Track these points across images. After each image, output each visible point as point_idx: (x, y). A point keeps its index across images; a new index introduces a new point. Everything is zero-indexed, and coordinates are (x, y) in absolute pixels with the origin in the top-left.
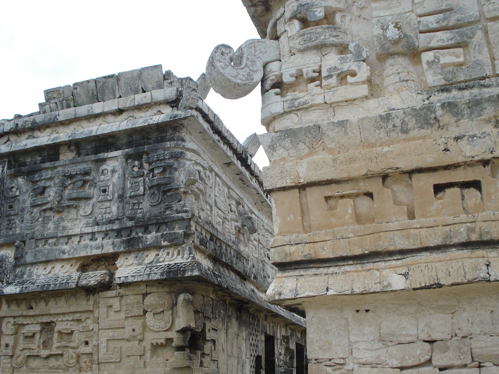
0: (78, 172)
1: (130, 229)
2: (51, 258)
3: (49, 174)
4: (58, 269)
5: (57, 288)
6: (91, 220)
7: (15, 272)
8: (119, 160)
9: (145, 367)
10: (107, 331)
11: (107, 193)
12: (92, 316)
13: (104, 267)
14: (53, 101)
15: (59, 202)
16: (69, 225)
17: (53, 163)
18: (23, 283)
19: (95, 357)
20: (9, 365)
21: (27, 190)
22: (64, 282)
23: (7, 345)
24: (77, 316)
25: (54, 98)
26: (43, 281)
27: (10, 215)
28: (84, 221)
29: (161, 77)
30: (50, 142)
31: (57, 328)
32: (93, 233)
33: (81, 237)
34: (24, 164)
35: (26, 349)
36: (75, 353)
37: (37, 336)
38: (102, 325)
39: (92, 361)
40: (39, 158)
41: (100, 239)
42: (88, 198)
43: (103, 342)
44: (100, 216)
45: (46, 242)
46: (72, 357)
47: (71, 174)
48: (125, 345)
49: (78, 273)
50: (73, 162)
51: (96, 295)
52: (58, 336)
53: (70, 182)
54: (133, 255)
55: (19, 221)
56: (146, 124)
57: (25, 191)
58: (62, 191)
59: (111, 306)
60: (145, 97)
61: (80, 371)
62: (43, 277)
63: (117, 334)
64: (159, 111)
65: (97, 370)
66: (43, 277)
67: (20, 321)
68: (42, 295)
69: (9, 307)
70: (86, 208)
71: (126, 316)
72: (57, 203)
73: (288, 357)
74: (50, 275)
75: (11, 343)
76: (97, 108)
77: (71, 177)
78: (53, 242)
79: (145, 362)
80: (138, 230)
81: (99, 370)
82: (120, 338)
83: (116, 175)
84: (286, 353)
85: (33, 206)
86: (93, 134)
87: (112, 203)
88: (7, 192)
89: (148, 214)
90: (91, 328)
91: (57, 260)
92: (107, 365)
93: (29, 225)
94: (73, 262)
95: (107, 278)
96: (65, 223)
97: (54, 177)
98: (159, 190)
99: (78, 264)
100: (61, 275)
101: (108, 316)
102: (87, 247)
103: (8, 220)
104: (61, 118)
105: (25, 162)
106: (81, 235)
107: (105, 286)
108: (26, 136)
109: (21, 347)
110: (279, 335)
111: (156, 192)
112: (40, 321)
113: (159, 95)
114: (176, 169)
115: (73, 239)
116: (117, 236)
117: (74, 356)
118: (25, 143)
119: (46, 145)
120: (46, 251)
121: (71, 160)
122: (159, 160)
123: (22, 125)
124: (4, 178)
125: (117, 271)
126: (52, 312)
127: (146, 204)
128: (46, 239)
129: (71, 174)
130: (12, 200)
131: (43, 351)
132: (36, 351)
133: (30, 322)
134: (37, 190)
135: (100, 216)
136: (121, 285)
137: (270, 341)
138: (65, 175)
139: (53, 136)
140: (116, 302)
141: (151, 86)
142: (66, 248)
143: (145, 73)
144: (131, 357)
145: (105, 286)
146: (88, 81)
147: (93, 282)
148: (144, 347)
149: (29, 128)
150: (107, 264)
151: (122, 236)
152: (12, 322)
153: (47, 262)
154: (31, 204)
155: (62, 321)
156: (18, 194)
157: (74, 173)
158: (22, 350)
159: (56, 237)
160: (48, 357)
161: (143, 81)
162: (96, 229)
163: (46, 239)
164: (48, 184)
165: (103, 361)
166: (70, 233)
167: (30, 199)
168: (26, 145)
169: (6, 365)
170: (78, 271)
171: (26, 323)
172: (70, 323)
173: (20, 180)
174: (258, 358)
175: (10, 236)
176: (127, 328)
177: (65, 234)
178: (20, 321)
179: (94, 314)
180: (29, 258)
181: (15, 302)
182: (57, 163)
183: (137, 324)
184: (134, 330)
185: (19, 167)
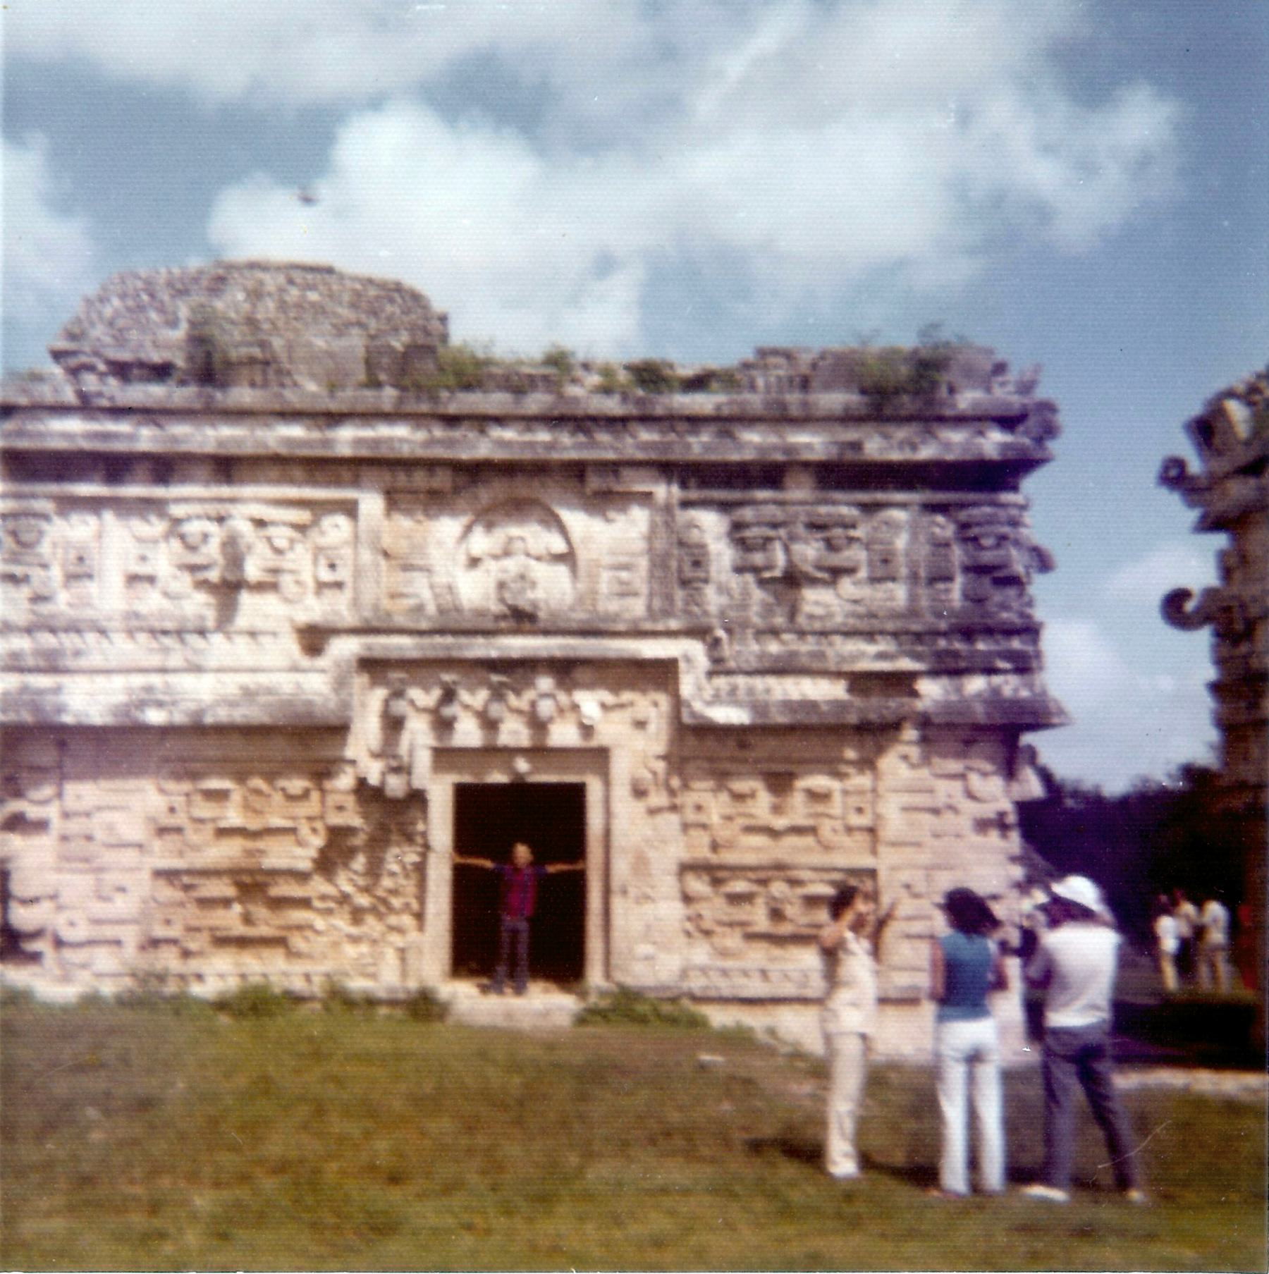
48: (927, 818)
126: (795, 755)
183: (957, 786)
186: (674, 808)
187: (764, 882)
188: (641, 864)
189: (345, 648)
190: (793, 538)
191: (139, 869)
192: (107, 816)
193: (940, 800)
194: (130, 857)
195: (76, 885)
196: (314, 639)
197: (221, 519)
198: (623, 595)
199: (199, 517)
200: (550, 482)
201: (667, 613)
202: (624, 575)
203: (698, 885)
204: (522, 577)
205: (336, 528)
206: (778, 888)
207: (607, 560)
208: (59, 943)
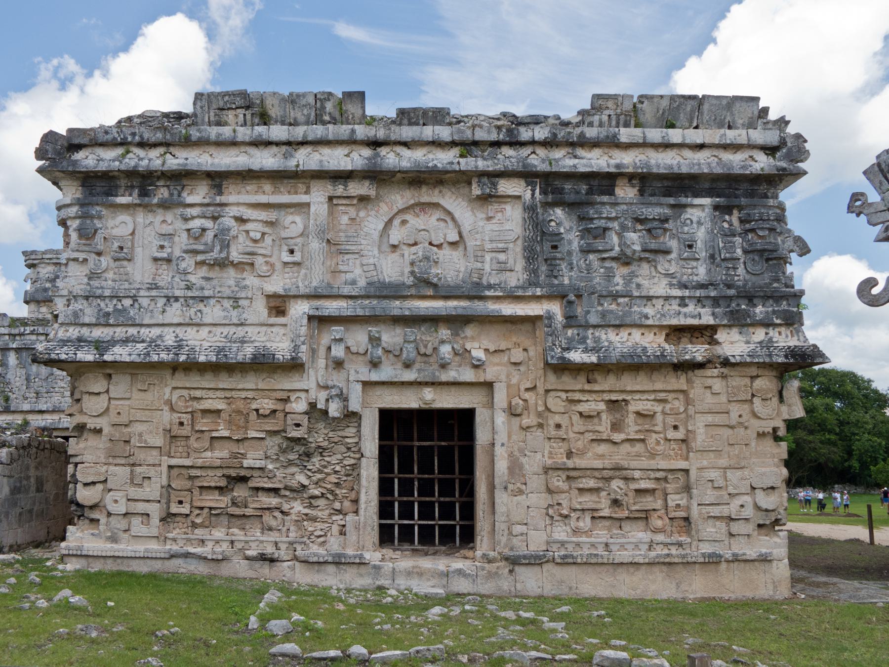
1: (731, 298)
2: (628, 322)
8: (707, 210)
11: (694, 250)
14: (607, 112)
20: (562, 450)
21: (571, 228)
24: (662, 395)
25: (607, 108)
27: (555, 259)
28: (665, 281)
29: (756, 113)
31: (632, 408)
32: (682, 298)
35: (590, 431)
37: (604, 416)
42: (667, 252)
53: (639, 227)
54: (735, 331)
55: (566, 268)
56: (748, 172)
60: (739, 136)
64: (751, 157)
66: (619, 345)
67: (577, 396)
70: (664, 265)
76: (675, 135)
80: (740, 301)
83: (703, 229)
86: (676, 170)
87: (700, 262)
89: (750, 283)
90: (682, 410)
96: (639, 280)
98: (761, 256)
99: (664, 333)
102: (679, 313)
104: (623, 139)
105: (563, 189)
106: (667, 298)
111: (757, 258)
112: (607, 398)
113: (759, 136)
114: (780, 233)
115: (654, 301)
122: (761, 220)
123: (563, 137)
124: (536, 206)
126: (629, 388)
127: (741, 271)
128: (615, 296)
133: (590, 399)
139: (612, 162)
141: (741, 121)
142: (649, 310)
143: (738, 105)
146: (662, 97)
151: (719, 306)
152: (565, 398)
154: (580, 247)
157: (651, 217)
158: (582, 433)
161: (732, 114)
162: (687, 293)
163: (615, 296)
166: (651, 294)
167: (577, 239)
168: (575, 166)
171: (585, 399)
173: (559, 211)
178: (577, 396)
186: (540, 426)
187: (608, 479)
189: (300, 309)
190: (624, 228)
192: (138, 428)
193: (734, 418)
194: (152, 457)
195: (119, 473)
196: (278, 305)
197: (215, 218)
198: (501, 270)
199: (198, 217)
200: (445, 190)
201: (532, 284)
202: (502, 257)
203: (558, 481)
204: (427, 258)
205: (294, 223)
206: (616, 484)
207: (488, 246)
208: (109, 514)
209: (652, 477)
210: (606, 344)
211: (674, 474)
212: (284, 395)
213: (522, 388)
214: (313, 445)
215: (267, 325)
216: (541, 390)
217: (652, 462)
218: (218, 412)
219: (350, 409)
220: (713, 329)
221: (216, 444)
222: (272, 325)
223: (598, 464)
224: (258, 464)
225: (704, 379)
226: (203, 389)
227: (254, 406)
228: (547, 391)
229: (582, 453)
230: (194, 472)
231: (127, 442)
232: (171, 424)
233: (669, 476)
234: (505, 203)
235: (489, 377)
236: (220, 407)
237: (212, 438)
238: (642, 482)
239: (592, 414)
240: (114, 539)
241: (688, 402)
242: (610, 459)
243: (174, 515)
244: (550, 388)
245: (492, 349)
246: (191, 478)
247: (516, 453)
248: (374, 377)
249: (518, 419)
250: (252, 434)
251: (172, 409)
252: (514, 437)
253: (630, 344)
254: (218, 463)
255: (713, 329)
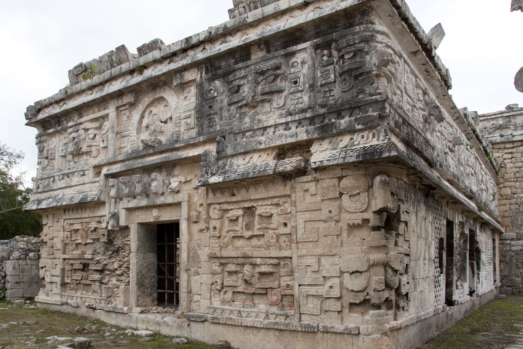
0: (269, 68)
2: (249, 149)
3: (243, 73)
4: (256, 158)
5: (255, 175)
6: (284, 111)
7: (218, 164)
9: (342, 246)
10: (304, 213)
12: (289, 200)
13: (298, 154)
15: (253, 97)
16: (263, 118)
17: (245, 62)
18: (225, 173)
19: (294, 237)
20: (217, 245)
21: (224, 91)
22: (262, 169)
23: (215, 228)
24: (275, 201)
26: (242, 170)
27: (210, 115)
28: (278, 113)
30: (241, 44)
32: (287, 123)
33: (275, 128)
34: (220, 68)
35: (231, 231)
36: (275, 233)
37: (240, 219)
38: (299, 208)
39: (291, 241)
40: (233, 61)
41: (293, 129)
42: (280, 91)
43: (301, 223)
44: (293, 106)
45: (244, 135)
46: (272, 237)
47: (262, 70)
48: (322, 225)
49: (275, 161)
50: (264, 60)
51: (292, 180)
52: (259, 219)
53: (262, 78)
57: (222, 92)
58: (255, 87)
59: (307, 190)
61: (280, 250)
62: (243, 167)
63: (314, 215)
65: (296, 248)
66: (243, 167)
67: (225, 206)
68: (243, 183)
69: (214, 195)
70: (278, 101)
71: (323, 199)
72: (251, 98)
73: (462, 241)
74: (249, 164)
75: (218, 226)
77: (262, 73)
78: (250, 135)
79: (342, 241)
81: (298, 248)
82: (317, 219)
84: (460, 237)
85: (230, 105)
88: (207, 94)
90: (289, 211)
91: (255, 151)
92: (305, 244)
93: (227, 121)
94: (269, 152)
95: (303, 164)
97: (247, 75)
99: (274, 153)
100: (259, 163)
101: (304, 199)
102: (282, 136)
103: (209, 119)
105: (220, 66)
106: (276, 126)
107: (300, 172)
108: (220, 42)
109: (226, 229)
110: (457, 220)
112: (242, 206)
115: (268, 130)
116: (310, 124)
117: (274, 236)
118: (220, 47)
119: (238, 46)
120: (244, 143)
121: (261, 58)
124: (203, 83)
125: (312, 157)
126: (252, 198)
128: (244, 133)
129: (262, 70)
130: (211, 101)
131: (246, 232)
132: (240, 232)
133: (233, 208)
134: (232, 89)
135: (293, 106)
136: (316, 170)
137: (450, 225)
138: (257, 73)
140: (312, 187)
142: (263, 139)
144: (329, 237)
145: (300, 172)
147: (289, 168)
148: (341, 227)
149: (221, 34)
150: (301, 152)
153: (246, 153)
154: (228, 102)
155: (262, 205)
156: (216, 95)
157: (265, 69)
158: (228, 232)
159: (252, 130)
160: (251, 238)
162: (289, 119)
163: (243, 133)
164: (242, 82)
165: (301, 240)
166: (265, 125)
168: (219, 50)
169: (215, 245)
170: (274, 159)
171: (230, 208)
172: (268, 207)
173: (217, 83)
174: (441, 240)
175: (211, 133)
176: (323, 210)
177: (260, 126)
178: (225, 206)
179: (291, 198)
180: (229, 151)
181: (219, 191)
182: (249, 63)
183: (334, 206)
184: (330, 212)
185: (215, 71)
188: (194, 257)
189: (104, 171)
191: (59, 258)
205: (107, 125)
209: (268, 263)
210: (235, 167)
211: (285, 261)
212: (97, 219)
213: (198, 205)
214: (117, 246)
215: (92, 182)
216: (205, 205)
217: (268, 252)
218: (78, 230)
219: (120, 225)
220: (309, 143)
221: (79, 246)
222: (95, 182)
223: (234, 254)
224: (90, 257)
225: (303, 184)
226: (73, 219)
227: (89, 226)
228: (209, 205)
229: (226, 246)
230: (72, 262)
231: (53, 247)
232: (64, 238)
233: (281, 263)
234: (191, 86)
235: (179, 200)
236: (78, 228)
237: (77, 244)
238: (263, 267)
239: (233, 218)
240: (48, 295)
241: (294, 204)
242: (242, 250)
243: (67, 283)
244: (209, 202)
245: (183, 180)
246: (72, 265)
247: (196, 248)
248: (133, 204)
249: (197, 224)
250: (89, 241)
251: (64, 230)
252: (196, 237)
253: (249, 164)
254: (77, 257)
255: (309, 143)
